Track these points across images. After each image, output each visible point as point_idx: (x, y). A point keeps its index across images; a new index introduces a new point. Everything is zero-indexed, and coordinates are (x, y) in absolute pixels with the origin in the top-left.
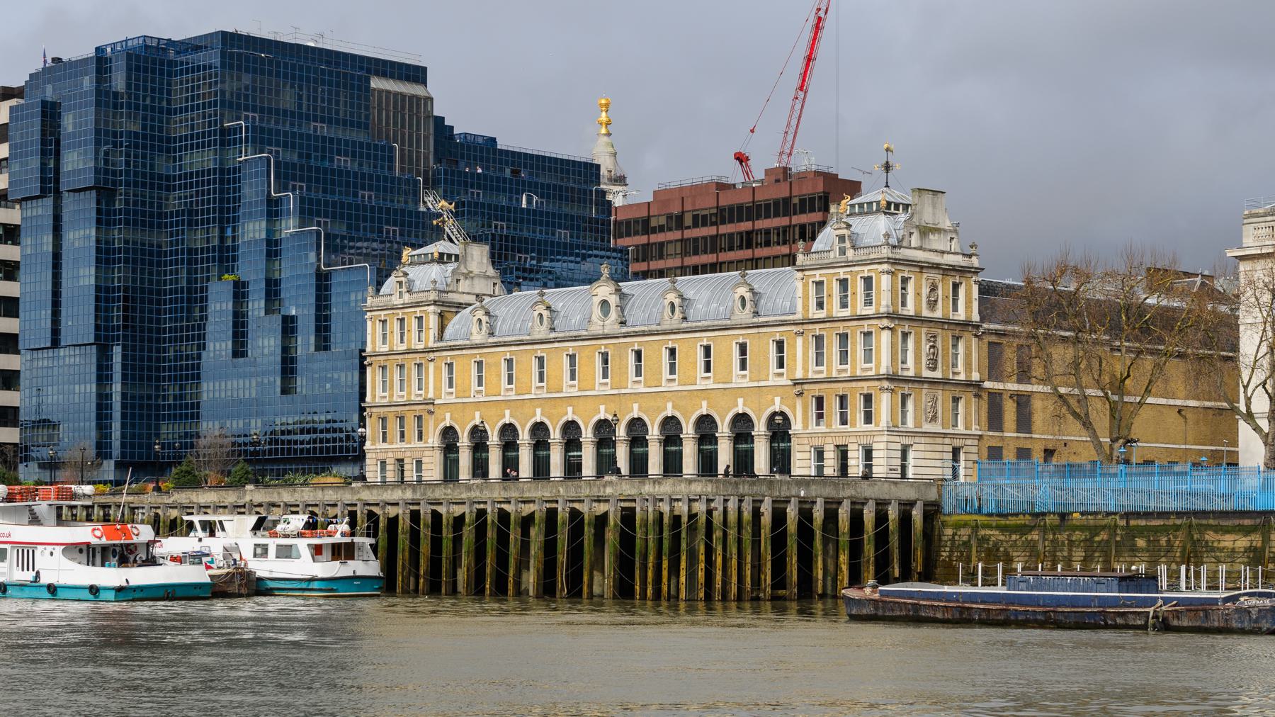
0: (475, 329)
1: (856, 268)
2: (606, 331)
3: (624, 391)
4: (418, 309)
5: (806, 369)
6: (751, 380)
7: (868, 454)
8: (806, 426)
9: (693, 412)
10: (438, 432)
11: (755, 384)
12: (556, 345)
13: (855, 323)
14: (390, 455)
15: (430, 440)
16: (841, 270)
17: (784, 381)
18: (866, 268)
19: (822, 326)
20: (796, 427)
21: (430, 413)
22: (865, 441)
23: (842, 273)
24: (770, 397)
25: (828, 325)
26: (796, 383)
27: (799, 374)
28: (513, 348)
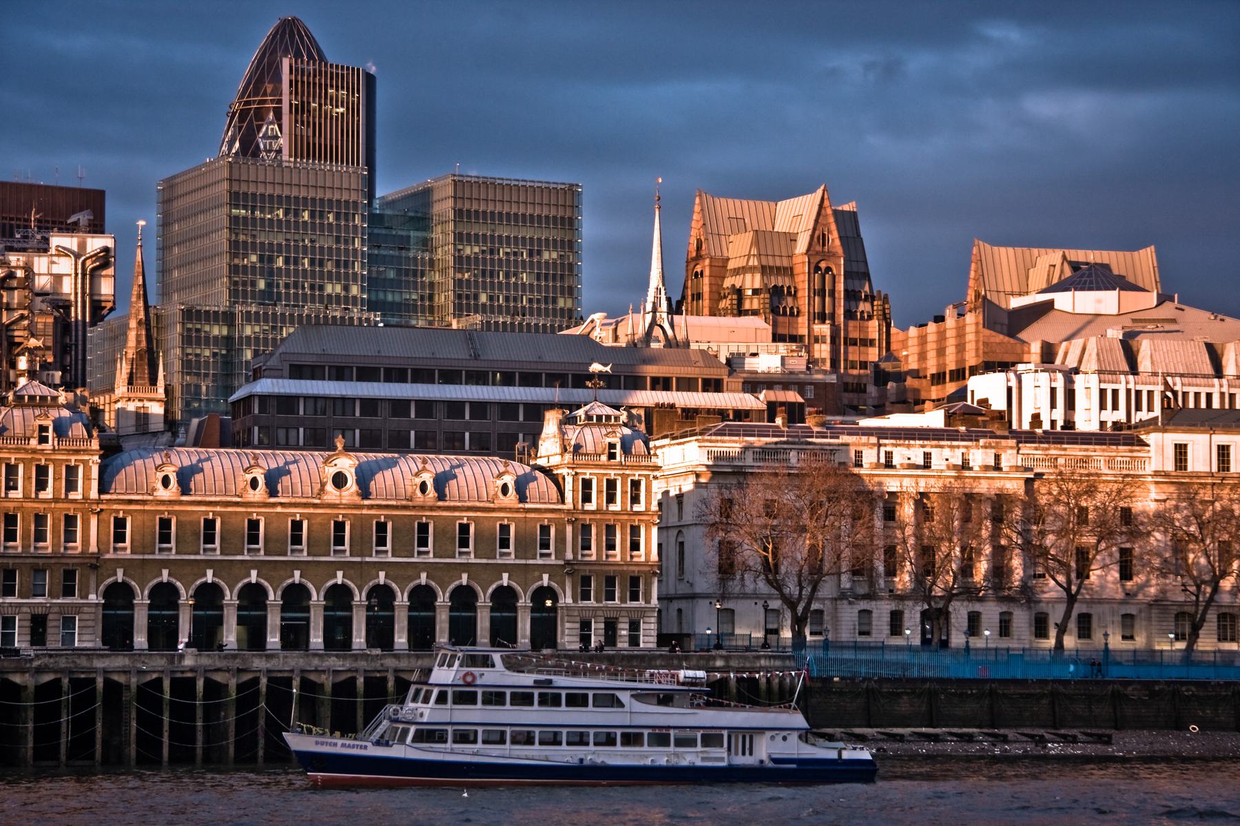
0: (159, 485)
1: (627, 472)
2: (344, 502)
3: (368, 559)
4: (73, 458)
5: (575, 553)
6: (516, 557)
7: (634, 626)
8: (575, 601)
9: (450, 583)
10: (102, 588)
11: (523, 562)
12: (279, 509)
13: (626, 517)
14: (25, 609)
15: (93, 598)
16: (612, 472)
17: (552, 560)
18: (637, 473)
19: (592, 517)
20: (567, 599)
21: (94, 567)
22: (635, 616)
23: (612, 474)
24: (537, 574)
25: (598, 517)
26: (568, 563)
27: (569, 555)
28: (218, 509)
